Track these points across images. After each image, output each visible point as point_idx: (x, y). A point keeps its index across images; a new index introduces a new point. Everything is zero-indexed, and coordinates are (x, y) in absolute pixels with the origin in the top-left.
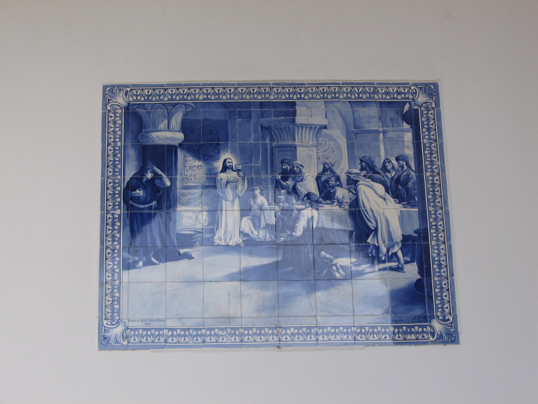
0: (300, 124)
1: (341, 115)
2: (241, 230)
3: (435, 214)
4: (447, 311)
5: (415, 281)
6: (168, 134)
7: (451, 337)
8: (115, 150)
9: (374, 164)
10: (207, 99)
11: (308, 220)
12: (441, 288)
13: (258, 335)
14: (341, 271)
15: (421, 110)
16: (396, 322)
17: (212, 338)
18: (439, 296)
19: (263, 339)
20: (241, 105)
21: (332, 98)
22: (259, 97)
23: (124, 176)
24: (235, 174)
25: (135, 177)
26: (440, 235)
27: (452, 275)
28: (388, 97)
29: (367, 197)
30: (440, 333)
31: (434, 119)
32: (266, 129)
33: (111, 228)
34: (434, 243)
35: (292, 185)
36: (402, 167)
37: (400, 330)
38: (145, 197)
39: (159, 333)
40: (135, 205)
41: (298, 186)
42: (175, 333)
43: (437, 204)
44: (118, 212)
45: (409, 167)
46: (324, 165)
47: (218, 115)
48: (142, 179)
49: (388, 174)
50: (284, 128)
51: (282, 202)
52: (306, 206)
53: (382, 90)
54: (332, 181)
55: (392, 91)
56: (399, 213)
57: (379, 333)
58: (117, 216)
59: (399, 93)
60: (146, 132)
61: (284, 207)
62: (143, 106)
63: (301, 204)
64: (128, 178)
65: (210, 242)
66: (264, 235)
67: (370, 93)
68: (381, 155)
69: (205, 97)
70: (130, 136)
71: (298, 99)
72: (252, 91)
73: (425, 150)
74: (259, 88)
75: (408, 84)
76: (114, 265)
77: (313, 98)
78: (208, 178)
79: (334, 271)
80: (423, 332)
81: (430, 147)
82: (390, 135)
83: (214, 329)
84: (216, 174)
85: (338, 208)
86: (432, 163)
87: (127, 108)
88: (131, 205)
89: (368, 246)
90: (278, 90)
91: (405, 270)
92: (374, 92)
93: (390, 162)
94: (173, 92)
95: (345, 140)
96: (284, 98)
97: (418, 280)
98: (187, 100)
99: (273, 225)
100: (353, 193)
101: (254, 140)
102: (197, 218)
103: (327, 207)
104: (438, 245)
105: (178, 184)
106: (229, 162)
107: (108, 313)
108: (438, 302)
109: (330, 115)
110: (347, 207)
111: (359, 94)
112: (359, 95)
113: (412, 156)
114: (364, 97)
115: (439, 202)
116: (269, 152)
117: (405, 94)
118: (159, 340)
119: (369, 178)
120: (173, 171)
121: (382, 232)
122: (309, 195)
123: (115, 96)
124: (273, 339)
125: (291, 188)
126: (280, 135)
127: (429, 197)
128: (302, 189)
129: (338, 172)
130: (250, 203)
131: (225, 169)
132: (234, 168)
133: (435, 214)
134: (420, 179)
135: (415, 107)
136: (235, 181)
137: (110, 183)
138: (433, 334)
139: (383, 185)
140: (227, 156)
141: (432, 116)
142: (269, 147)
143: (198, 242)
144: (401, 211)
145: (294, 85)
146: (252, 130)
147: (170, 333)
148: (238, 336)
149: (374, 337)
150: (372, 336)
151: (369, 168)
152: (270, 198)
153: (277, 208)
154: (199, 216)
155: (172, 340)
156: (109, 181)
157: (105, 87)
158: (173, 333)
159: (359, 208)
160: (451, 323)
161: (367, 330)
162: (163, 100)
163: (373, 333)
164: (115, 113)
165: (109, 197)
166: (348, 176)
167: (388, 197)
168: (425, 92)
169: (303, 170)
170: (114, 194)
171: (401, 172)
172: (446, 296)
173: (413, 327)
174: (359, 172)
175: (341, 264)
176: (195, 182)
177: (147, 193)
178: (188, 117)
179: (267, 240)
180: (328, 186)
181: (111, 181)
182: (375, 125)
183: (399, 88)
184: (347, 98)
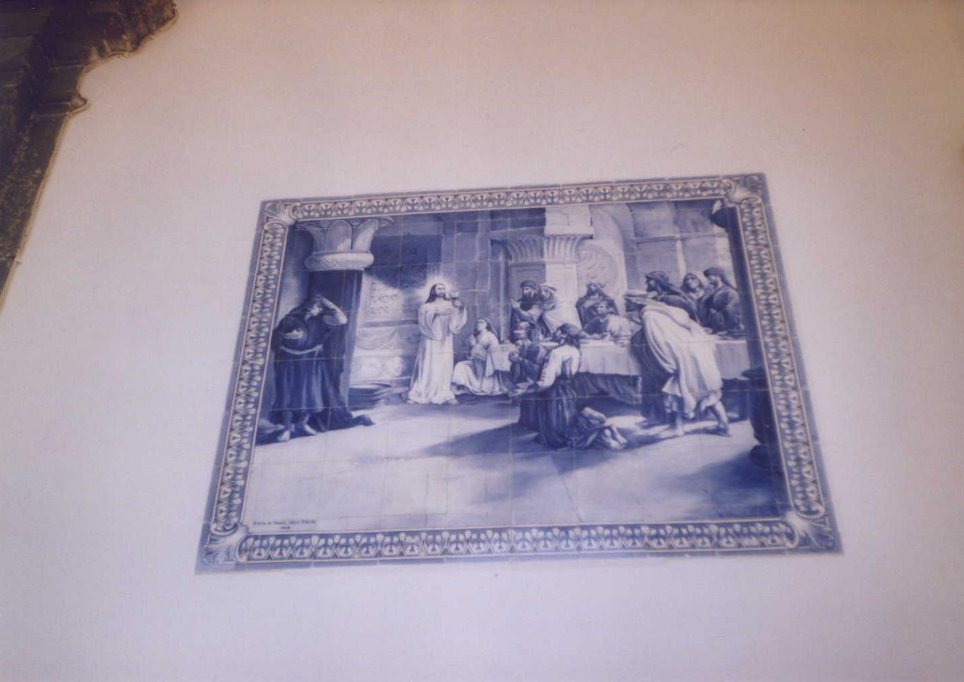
0: (552, 235)
2: (454, 381)
3: (776, 347)
6: (350, 255)
8: (267, 279)
10: (413, 210)
11: (564, 364)
12: (798, 460)
14: (619, 437)
16: (721, 516)
22: (490, 205)
25: (292, 313)
27: (815, 438)
28: (687, 195)
30: (804, 535)
31: (762, 218)
34: (777, 390)
36: (715, 284)
40: (288, 351)
44: (261, 362)
45: (726, 283)
46: (589, 286)
47: (429, 229)
48: (305, 314)
49: (692, 294)
51: (522, 339)
53: (677, 186)
54: (602, 307)
56: (715, 348)
57: (689, 535)
59: (703, 189)
60: (318, 255)
61: (523, 346)
62: (317, 224)
63: (551, 341)
64: (282, 315)
65: (402, 398)
66: (491, 386)
67: (659, 192)
68: (678, 270)
69: (410, 208)
71: (548, 204)
72: (480, 198)
75: (717, 177)
76: (243, 438)
77: (571, 202)
79: (606, 436)
80: (772, 533)
81: (758, 255)
82: (693, 242)
83: (397, 533)
84: (419, 305)
85: (612, 344)
87: (293, 228)
88: (283, 351)
89: (664, 396)
92: (665, 190)
93: (694, 278)
97: (756, 448)
98: (382, 213)
102: (383, 365)
104: (785, 393)
106: (440, 289)
107: (222, 511)
108: (794, 483)
110: (627, 342)
111: (641, 193)
116: (502, 273)
117: (713, 189)
119: (662, 300)
120: (353, 305)
122: (564, 328)
128: (554, 320)
129: (611, 295)
130: (469, 343)
131: (433, 297)
132: (447, 296)
133: (776, 347)
135: (731, 205)
136: (448, 314)
137: (254, 323)
138: (791, 536)
140: (439, 280)
142: (502, 266)
143: (382, 401)
144: (717, 346)
145: (544, 188)
147: (322, 542)
148: (438, 544)
153: (512, 348)
156: (254, 319)
158: (326, 541)
159: (646, 342)
160: (823, 517)
162: (347, 215)
163: (680, 535)
164: (274, 234)
166: (627, 300)
167: (695, 326)
168: (745, 185)
169: (556, 295)
170: (258, 337)
171: (713, 291)
173: (753, 524)
174: (643, 292)
178: (381, 234)
180: (594, 313)
182: (668, 231)
183: (703, 182)
184: (623, 199)
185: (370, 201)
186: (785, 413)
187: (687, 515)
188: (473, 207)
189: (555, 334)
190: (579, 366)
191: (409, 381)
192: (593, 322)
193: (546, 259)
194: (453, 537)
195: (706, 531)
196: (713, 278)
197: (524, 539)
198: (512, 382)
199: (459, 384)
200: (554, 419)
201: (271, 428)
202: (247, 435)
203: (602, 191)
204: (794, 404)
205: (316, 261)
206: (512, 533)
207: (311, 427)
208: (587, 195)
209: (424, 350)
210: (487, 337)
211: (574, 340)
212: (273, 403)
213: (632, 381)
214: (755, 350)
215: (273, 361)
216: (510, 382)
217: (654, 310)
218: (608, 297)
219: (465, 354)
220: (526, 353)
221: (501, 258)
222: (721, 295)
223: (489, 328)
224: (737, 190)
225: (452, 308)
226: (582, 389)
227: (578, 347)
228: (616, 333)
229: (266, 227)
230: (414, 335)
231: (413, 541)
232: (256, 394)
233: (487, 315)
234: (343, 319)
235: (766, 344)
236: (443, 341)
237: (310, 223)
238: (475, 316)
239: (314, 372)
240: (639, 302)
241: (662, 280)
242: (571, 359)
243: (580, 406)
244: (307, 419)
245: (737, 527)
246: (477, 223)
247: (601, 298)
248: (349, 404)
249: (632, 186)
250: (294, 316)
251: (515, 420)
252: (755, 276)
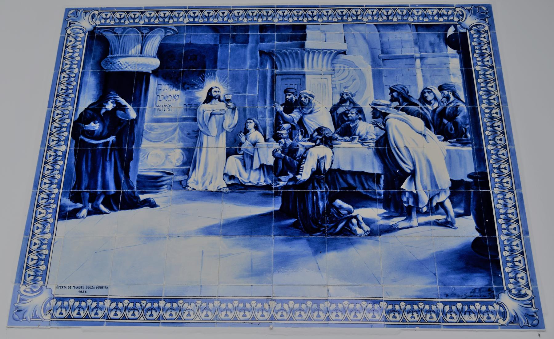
0: (311, 49)
1: (365, 38)
2: (226, 172)
4: (523, 282)
5: (472, 240)
6: (140, 59)
8: (70, 77)
9: (409, 94)
10: (194, 22)
11: (319, 161)
12: (512, 251)
13: (241, 310)
14: (363, 225)
15: (470, 33)
16: (447, 295)
17: (173, 313)
18: (509, 262)
19: (248, 317)
20: (235, 28)
21: (353, 21)
22: (260, 20)
23: (77, 106)
24: (223, 105)
26: (504, 181)
27: (527, 233)
28: (426, 20)
29: (399, 133)
30: (514, 314)
31: (489, 43)
32: (267, 55)
33: (50, 168)
34: (497, 191)
35: (298, 118)
36: (448, 98)
37: (454, 308)
38: (101, 131)
39: (98, 304)
40: (87, 140)
41: (306, 119)
42: (120, 305)
43: (499, 142)
44: (63, 148)
45: (457, 98)
46: (342, 95)
47: (207, 39)
48: (101, 110)
49: (427, 106)
50: (290, 53)
51: (284, 138)
52: (316, 143)
53: (418, 12)
54: (352, 113)
55: (431, 13)
56: (445, 153)
57: (420, 311)
58: (60, 153)
60: (112, 58)
61: (285, 143)
62: (112, 30)
63: (309, 141)
64: (81, 109)
65: (183, 185)
66: (258, 178)
67: (402, 16)
69: (191, 20)
70: (92, 62)
71: (309, 22)
72: (251, 14)
73: (477, 78)
74: (260, 10)
75: (453, 6)
76: (47, 213)
77: (328, 21)
78: (186, 110)
79: (353, 224)
80: (488, 311)
81: (484, 74)
82: (429, 61)
84: (197, 105)
85: (359, 145)
86: (488, 93)
87: (91, 33)
88: (82, 141)
89: (404, 192)
90: (283, 13)
91: (455, 225)
92: (408, 15)
93: (430, 91)
94: (152, 15)
95: (370, 67)
96: (291, 21)
97: (477, 239)
99: (270, 166)
100: (380, 128)
101: (251, 67)
102: (167, 156)
103: (344, 144)
106: (216, 91)
108: (508, 270)
109: (350, 40)
110: (373, 145)
111: (388, 17)
112: (388, 18)
113: (461, 85)
114: (395, 19)
115: (501, 140)
117: (448, 16)
118: (96, 314)
119: (402, 110)
120: (142, 102)
121: (422, 177)
122: (320, 130)
123: (79, 19)
124: (263, 316)
125: (296, 122)
126: (284, 61)
127: (487, 133)
129: (360, 103)
130: (240, 139)
131: (209, 98)
132: (222, 98)
133: (496, 154)
134: (474, 113)
135: (462, 31)
136: (222, 113)
137: (58, 114)
138: (504, 315)
139: (422, 119)
140: (213, 83)
141: (486, 40)
142: (269, 75)
143: (166, 186)
144: (448, 151)
145: (305, 8)
146: (248, 56)
148: (210, 310)
149: (413, 317)
150: (410, 315)
151: (402, 98)
152: (267, 133)
153: (276, 145)
154: (170, 154)
155: (116, 314)
156: (57, 112)
157: (67, 10)
158: (117, 305)
161: (403, 307)
163: (412, 311)
165: (54, 130)
166: (373, 108)
167: (430, 133)
168: (474, 14)
169: (313, 101)
170: (62, 127)
171: (446, 104)
172: (520, 261)
173: (473, 303)
174: (389, 103)
175: (365, 216)
176: (169, 114)
177: (104, 127)
178: (167, 42)
179: (261, 184)
180: (346, 119)
181: (59, 112)
182: (410, 50)
183: (440, 9)
184: (373, 20)
185: (157, 12)
186: (502, 211)
187: (418, 294)
188: (245, 21)
189: (312, 135)
190: (332, 163)
191: (189, 170)
192: (345, 127)
193: (306, 70)
194: (223, 306)
195: (434, 307)
196: (446, 93)
197: (282, 310)
198: (275, 174)
199: (230, 174)
200: (310, 208)
201: (70, 206)
202: (51, 211)
203: (355, 13)
204: (510, 203)
205: (111, 63)
206: (273, 304)
207: (105, 207)
208: (342, 16)
209: (201, 145)
210: (255, 135)
211: (328, 141)
212: (73, 185)
213: (375, 178)
214: (479, 156)
215: (73, 148)
216: (273, 175)
217: (395, 118)
218: (357, 105)
219: (236, 149)
220: (287, 151)
221: (268, 68)
222: (452, 107)
223: (256, 128)
224: (468, 17)
225: (226, 109)
226: (332, 183)
227: (331, 147)
228: (363, 137)
229: (69, 31)
230: (193, 131)
231: (189, 307)
232: (58, 177)
233: (256, 116)
234: (133, 114)
235: (489, 152)
236: (218, 137)
237: (107, 29)
238: (245, 116)
239: (108, 159)
240: (383, 111)
241: (403, 91)
242: (325, 157)
243: (332, 197)
244: (101, 200)
245: (459, 306)
246: (249, 35)
247: (352, 105)
248: (138, 188)
249: (380, 9)
250: (91, 110)
251: (278, 208)
252: (481, 93)
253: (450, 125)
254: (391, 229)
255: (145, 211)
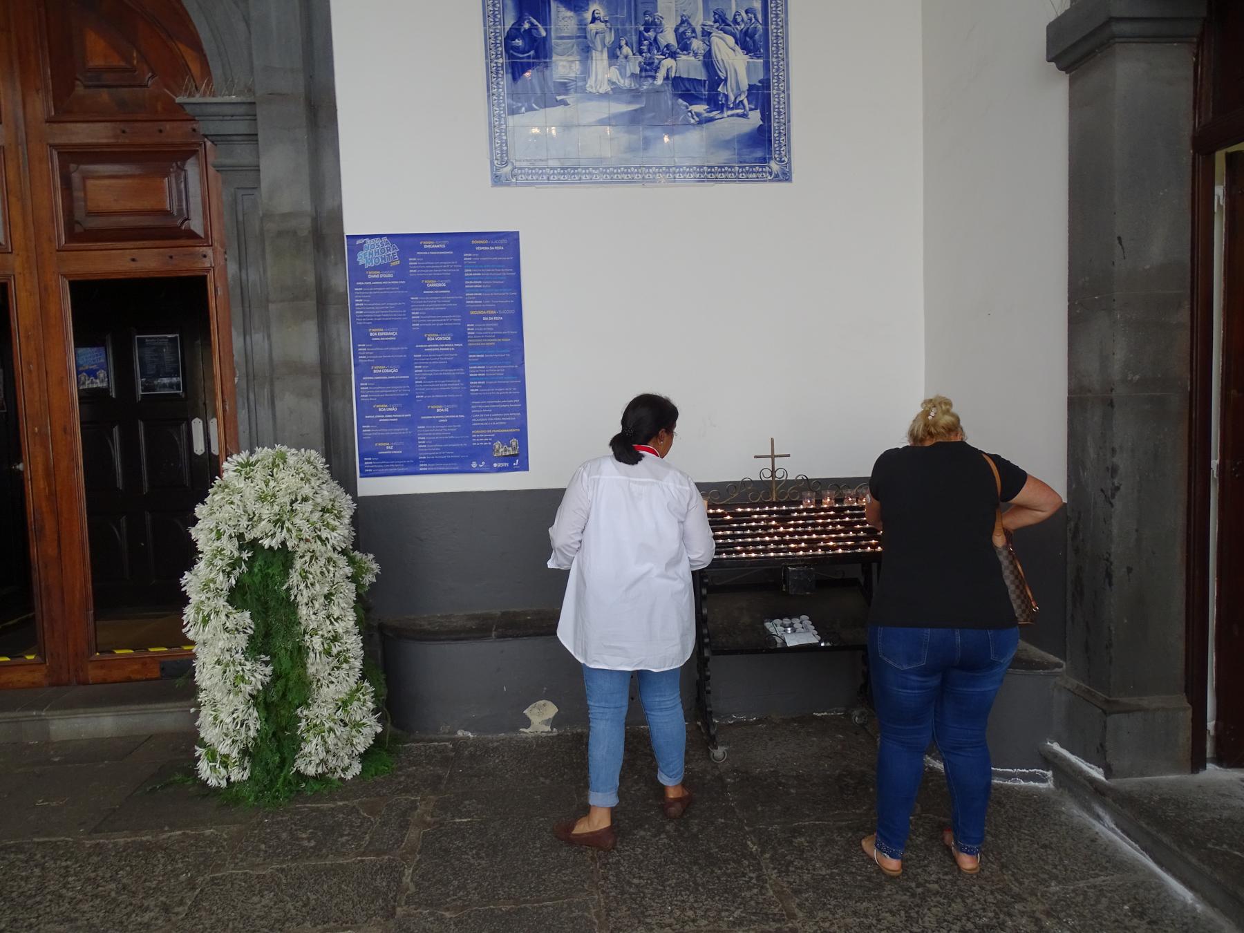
7: (785, 176)
44: (500, 61)
64: (508, 27)
65: (583, 90)
89: (719, 94)
103: (684, 57)
105: (553, 34)
122: (668, 46)
129: (693, 24)
131: (594, 20)
134: (766, 31)
138: (771, 174)
151: (721, 20)
153: (640, 59)
167: (738, 48)
210: (626, 50)
211: (673, 55)
214: (767, 66)
234: (544, 34)
253: (751, 43)
254: (711, 120)
255: (560, 108)
